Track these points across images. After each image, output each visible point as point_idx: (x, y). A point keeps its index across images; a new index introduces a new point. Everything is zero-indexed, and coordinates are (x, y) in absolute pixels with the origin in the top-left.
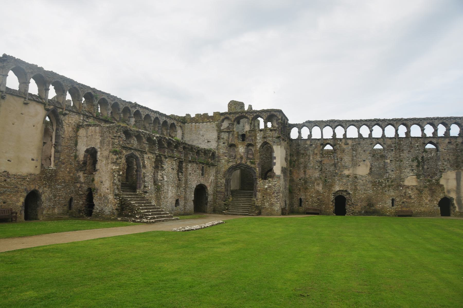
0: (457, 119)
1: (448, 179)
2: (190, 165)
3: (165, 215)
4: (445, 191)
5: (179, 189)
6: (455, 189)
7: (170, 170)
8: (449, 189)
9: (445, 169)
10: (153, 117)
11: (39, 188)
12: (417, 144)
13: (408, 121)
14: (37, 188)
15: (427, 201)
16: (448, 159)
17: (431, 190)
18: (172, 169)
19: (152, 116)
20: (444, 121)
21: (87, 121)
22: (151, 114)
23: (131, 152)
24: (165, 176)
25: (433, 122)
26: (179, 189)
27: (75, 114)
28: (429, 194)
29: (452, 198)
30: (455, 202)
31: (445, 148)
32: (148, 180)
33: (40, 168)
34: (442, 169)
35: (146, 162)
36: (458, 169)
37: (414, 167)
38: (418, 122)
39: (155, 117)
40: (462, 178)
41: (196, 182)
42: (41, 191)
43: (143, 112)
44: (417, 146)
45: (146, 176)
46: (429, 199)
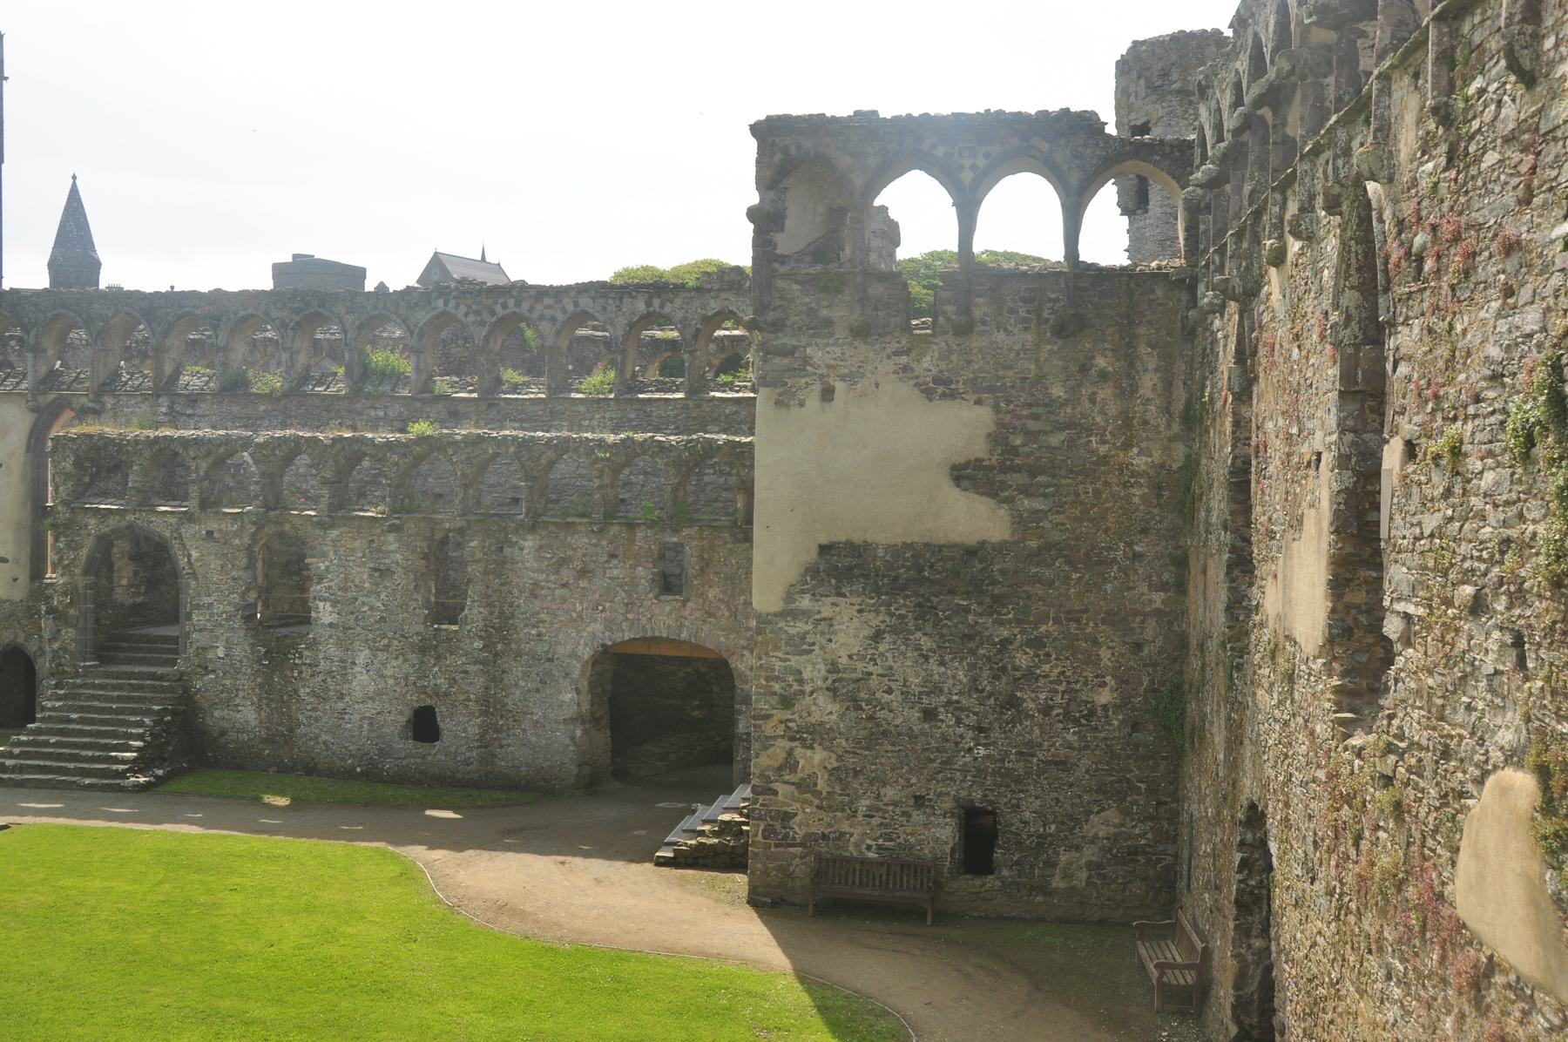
2: (530, 543)
3: (71, 766)
5: (438, 658)
7: (362, 576)
10: (553, 320)
11: (26, 640)
14: (20, 640)
18: (375, 570)
19: (542, 317)
21: (189, 412)
22: (531, 310)
23: (124, 523)
24: (321, 604)
26: (438, 658)
27: (140, 399)
32: (208, 620)
33: (28, 581)
35: (195, 554)
39: (561, 317)
41: (597, 627)
42: (32, 647)
43: (478, 313)
45: (198, 607)
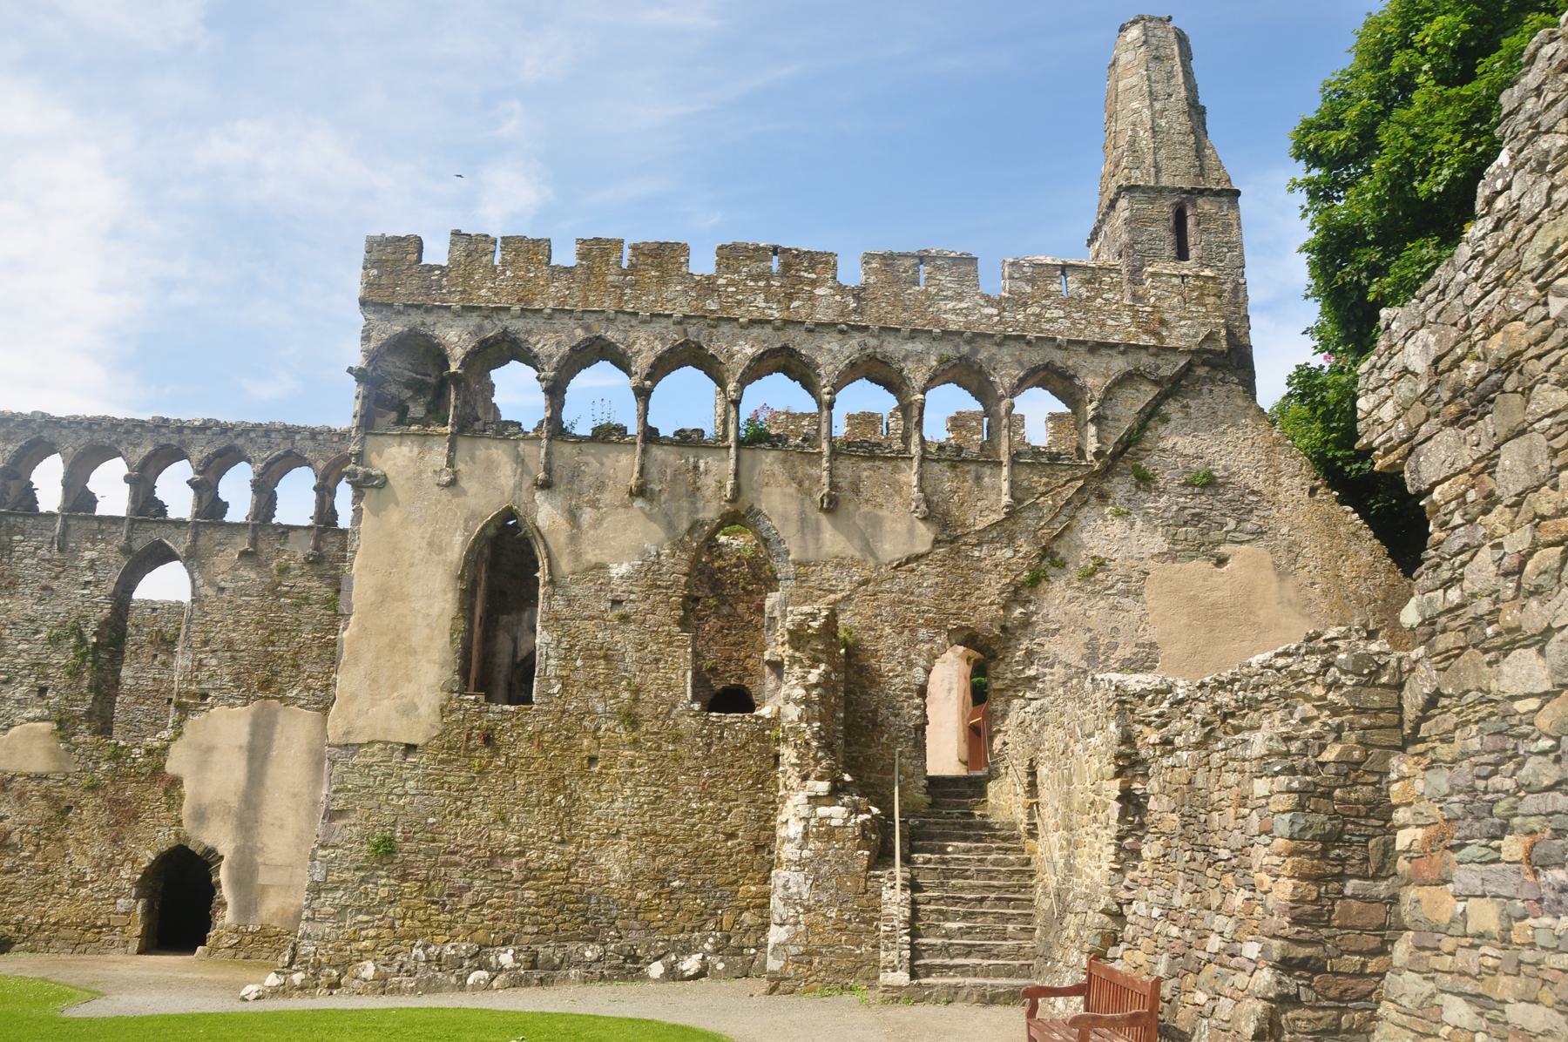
0: (298, 437)
1: (210, 750)
4: (186, 810)
6: (234, 802)
8: (206, 801)
9: (205, 696)
12: (88, 555)
13: (64, 432)
15: (82, 864)
16: (230, 644)
17: (115, 803)
20: (240, 442)
25: (182, 442)
28: (101, 827)
29: (211, 851)
30: (223, 875)
31: (223, 584)
34: (189, 694)
36: (267, 698)
37: (58, 678)
38: (114, 438)
40: (276, 745)
44: (92, 561)
46: (96, 852)
